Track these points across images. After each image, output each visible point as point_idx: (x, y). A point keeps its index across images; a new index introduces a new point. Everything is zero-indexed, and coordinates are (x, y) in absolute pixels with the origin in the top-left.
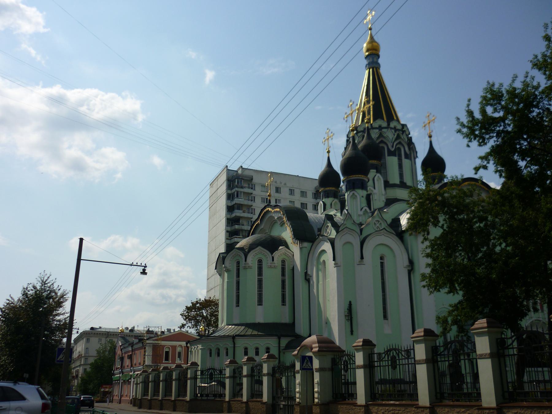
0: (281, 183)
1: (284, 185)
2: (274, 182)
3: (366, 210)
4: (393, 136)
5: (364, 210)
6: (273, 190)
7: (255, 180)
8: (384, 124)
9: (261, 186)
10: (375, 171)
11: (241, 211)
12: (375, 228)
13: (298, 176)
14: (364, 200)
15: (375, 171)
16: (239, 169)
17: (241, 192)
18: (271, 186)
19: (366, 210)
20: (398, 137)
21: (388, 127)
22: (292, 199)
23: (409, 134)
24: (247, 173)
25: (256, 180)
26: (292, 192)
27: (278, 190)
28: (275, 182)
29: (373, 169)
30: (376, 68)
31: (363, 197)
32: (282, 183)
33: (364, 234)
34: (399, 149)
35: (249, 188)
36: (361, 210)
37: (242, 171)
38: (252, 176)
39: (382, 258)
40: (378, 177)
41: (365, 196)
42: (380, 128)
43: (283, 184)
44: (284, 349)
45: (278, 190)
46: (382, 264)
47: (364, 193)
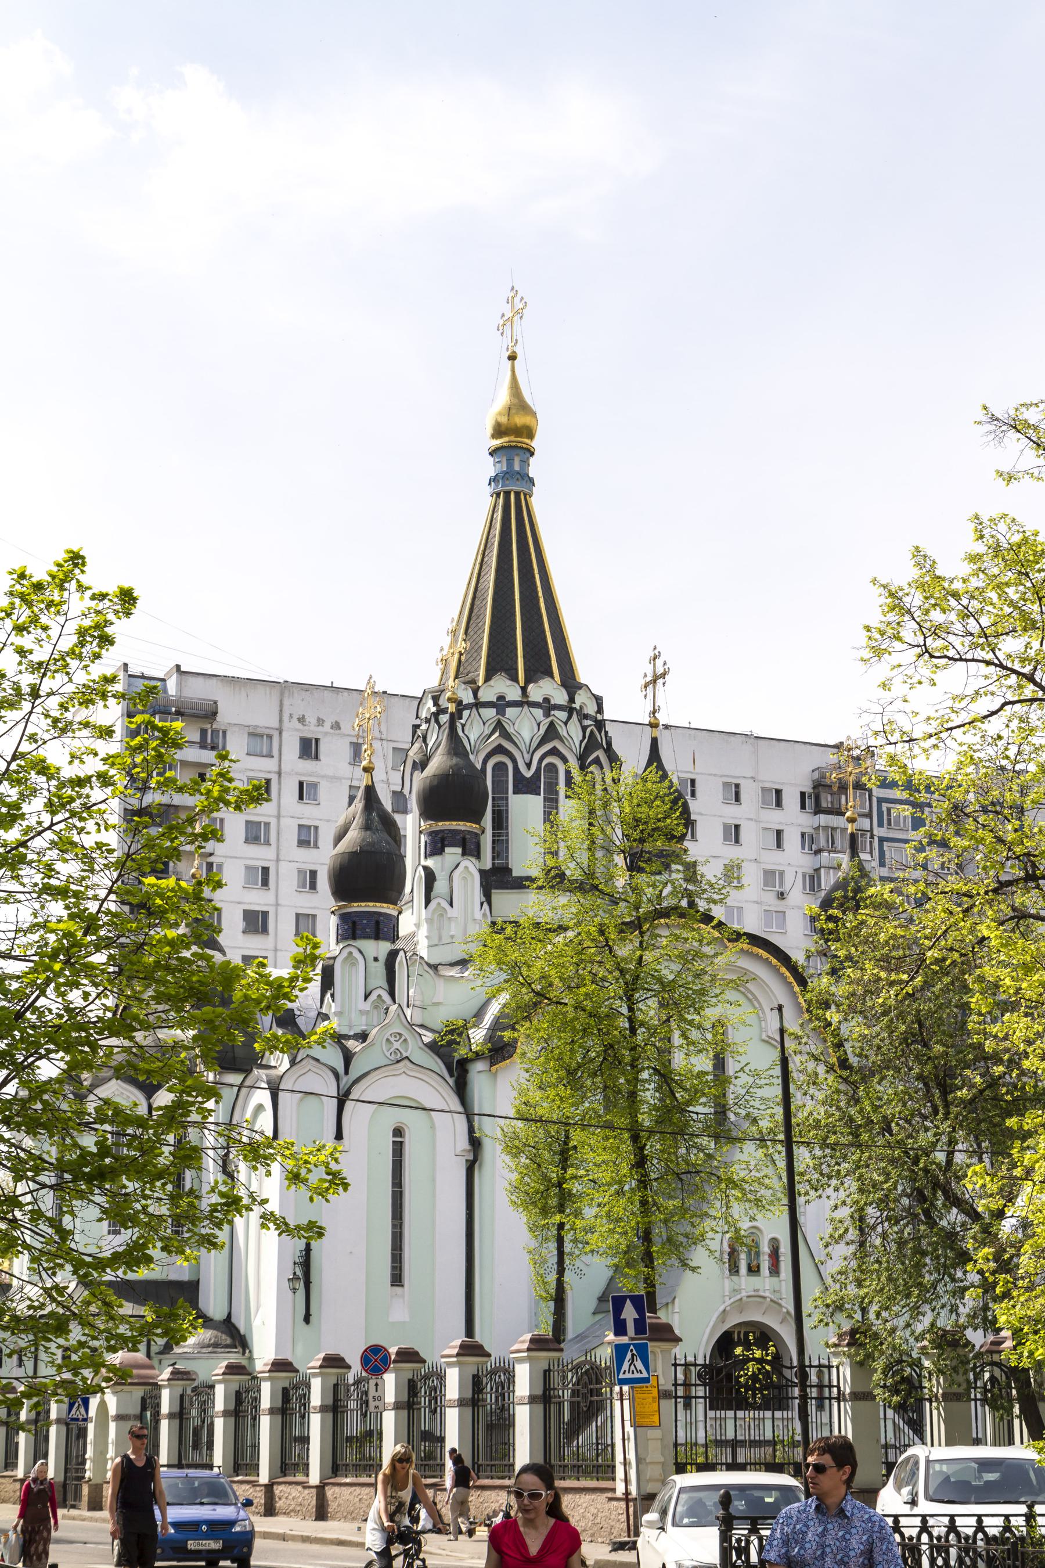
0: (320, 722)
1: (332, 728)
2: (295, 720)
3: (379, 996)
4: (536, 728)
5: (373, 997)
7: (224, 717)
8: (513, 693)
9: (250, 734)
10: (459, 850)
12: (388, 1054)
13: (385, 693)
14: (379, 970)
15: (459, 850)
16: (169, 674)
18: (284, 734)
19: (379, 996)
20: (551, 733)
21: (524, 702)
23: (600, 710)
24: (198, 692)
27: (309, 749)
28: (299, 719)
29: (452, 845)
30: (517, 494)
31: (376, 959)
32: (323, 721)
33: (355, 1072)
34: (552, 768)
35: (203, 745)
36: (366, 997)
37: (180, 685)
38: (215, 703)
39: (398, 1132)
40: (466, 867)
41: (382, 958)
42: (501, 704)
43: (327, 726)
44: (160, 1353)
45: (309, 749)
46: (398, 1149)
47: (383, 948)
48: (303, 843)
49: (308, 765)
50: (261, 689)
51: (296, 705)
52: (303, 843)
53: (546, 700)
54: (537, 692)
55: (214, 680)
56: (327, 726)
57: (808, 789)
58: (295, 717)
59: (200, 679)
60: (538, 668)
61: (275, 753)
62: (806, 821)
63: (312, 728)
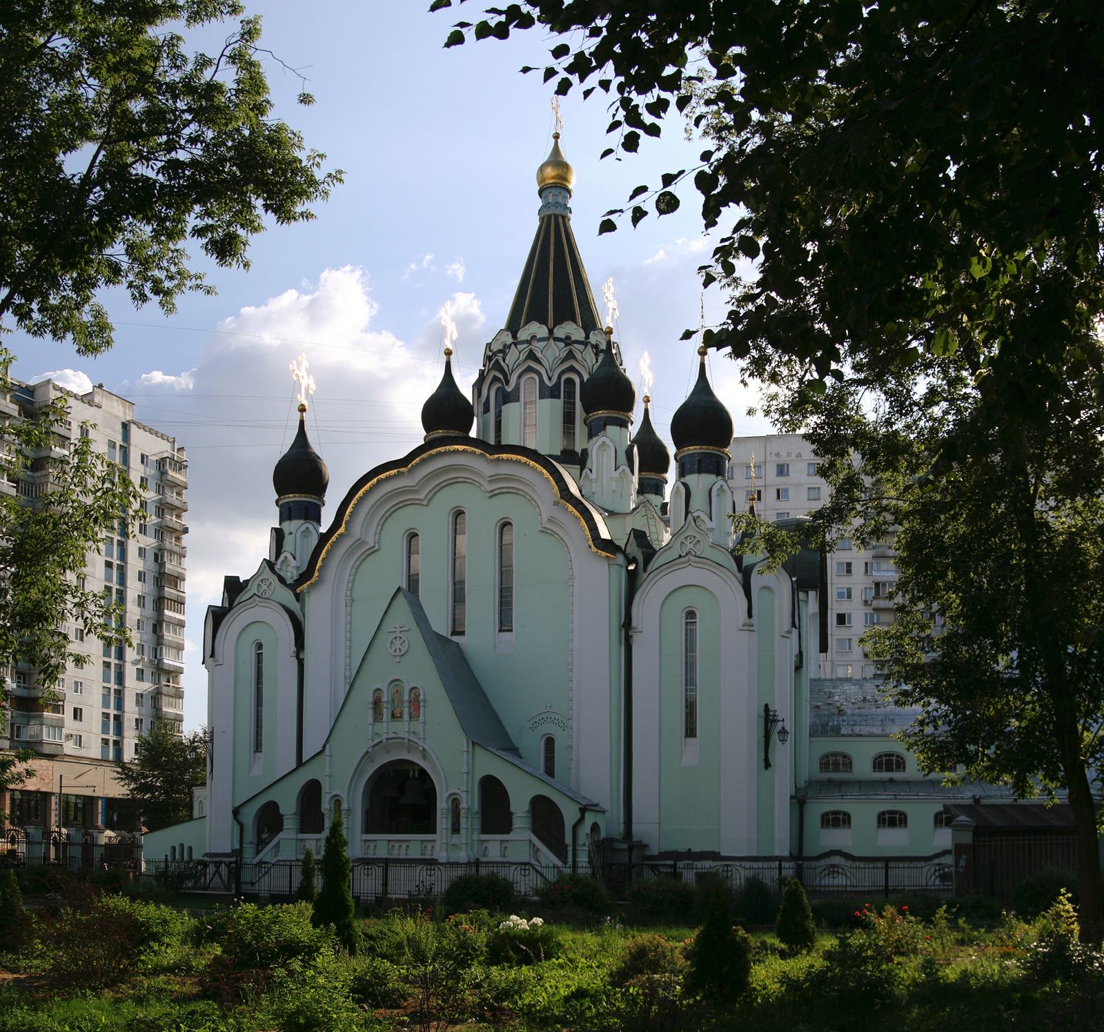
0: (789, 454)
2: (773, 456)
6: (771, 471)
27: (782, 470)
43: (794, 456)
45: (782, 470)
49: (782, 480)
53: (568, 338)
54: (560, 332)
60: (565, 314)
61: (763, 475)
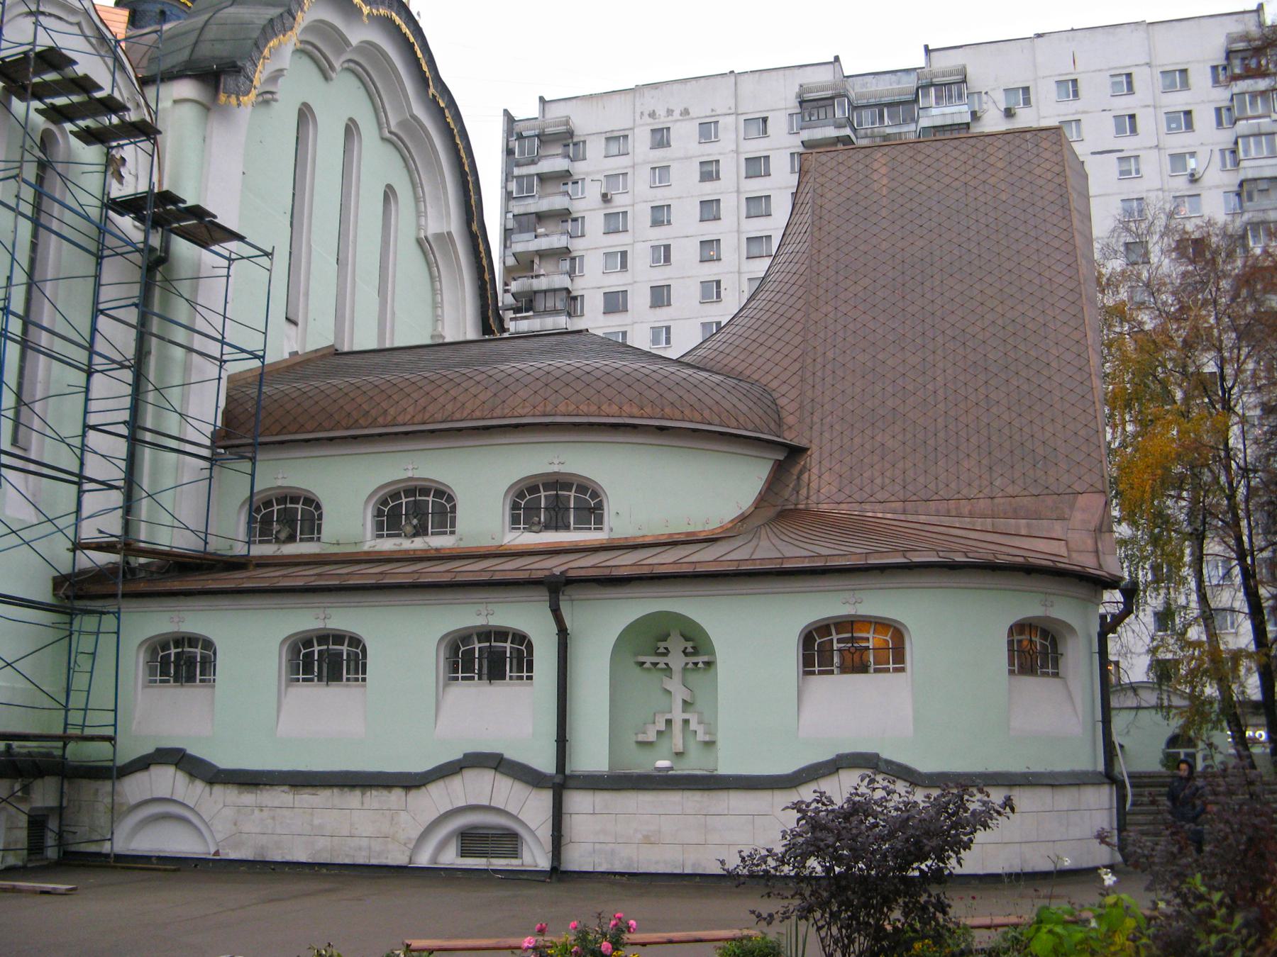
0: (670, 112)
1: (681, 115)
2: (646, 117)
6: (641, 141)
11: (531, 235)
13: (732, 72)
17: (530, 176)
22: (709, 155)
25: (583, 123)
26: (707, 130)
27: (661, 138)
28: (649, 115)
32: (672, 111)
43: (676, 115)
45: (661, 138)
48: (656, 223)
50: (616, 97)
51: (649, 102)
52: (656, 223)
55: (574, 101)
56: (676, 115)
57: (1221, 61)
58: (646, 113)
59: (562, 103)
61: (630, 150)
62: (1221, 96)
63: (662, 119)
